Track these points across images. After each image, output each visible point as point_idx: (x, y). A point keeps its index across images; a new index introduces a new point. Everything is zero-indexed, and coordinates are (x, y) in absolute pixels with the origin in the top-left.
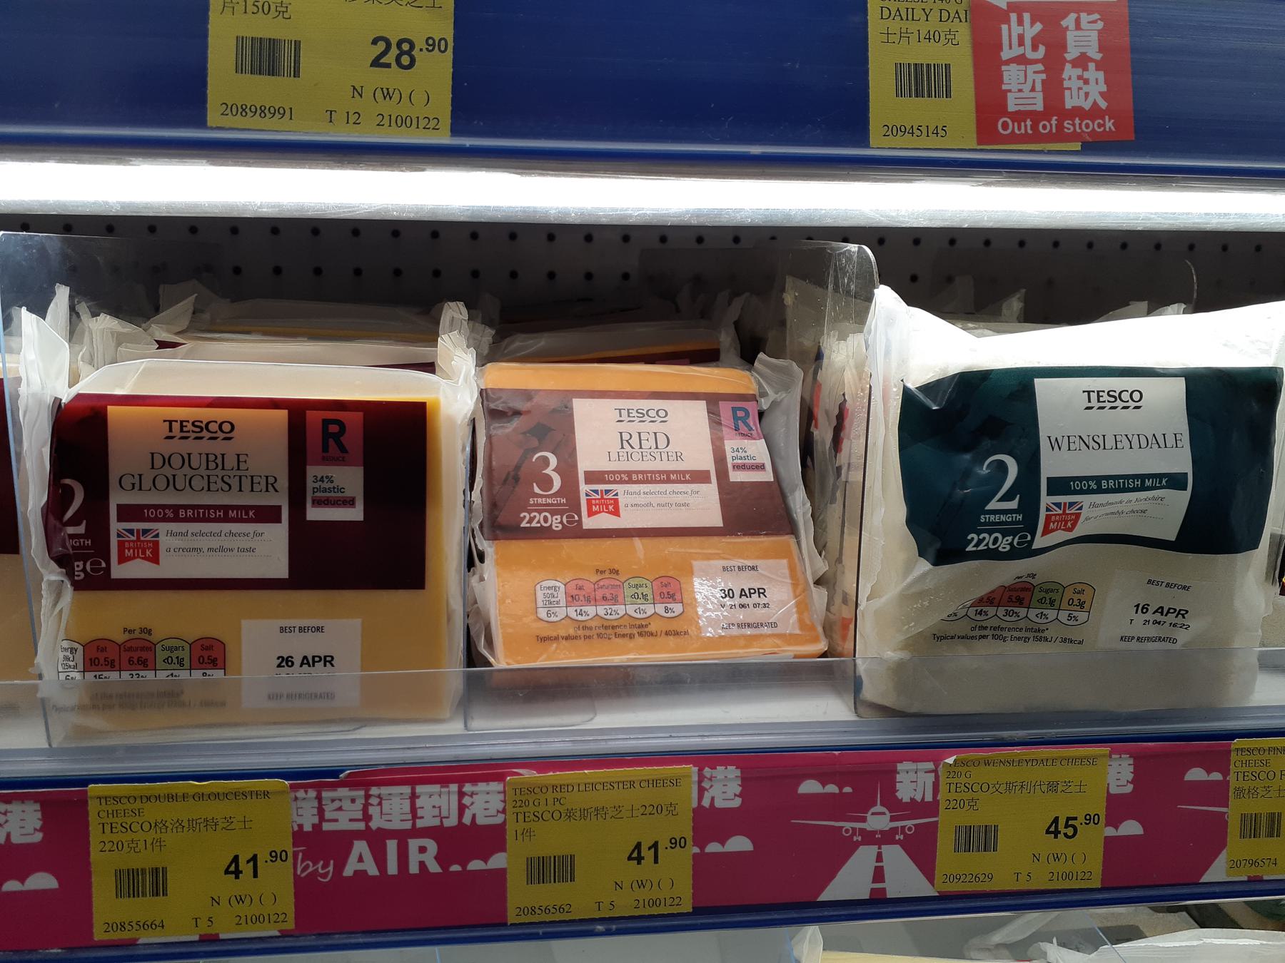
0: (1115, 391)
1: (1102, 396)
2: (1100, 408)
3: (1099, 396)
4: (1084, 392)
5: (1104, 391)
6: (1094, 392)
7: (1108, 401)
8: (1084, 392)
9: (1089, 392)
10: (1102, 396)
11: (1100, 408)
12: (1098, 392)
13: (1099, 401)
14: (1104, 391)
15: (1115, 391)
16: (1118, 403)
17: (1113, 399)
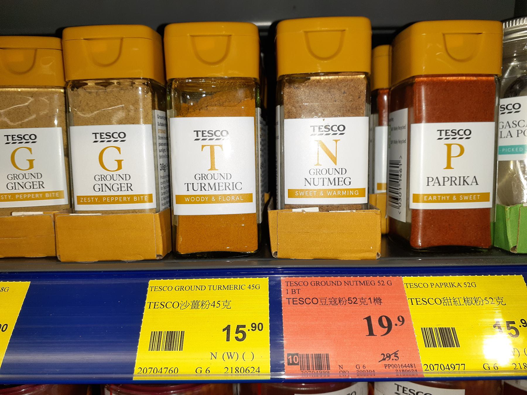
0: (212, 131)
1: (205, 134)
2: (203, 140)
3: (203, 134)
4: (194, 131)
5: (205, 131)
6: (200, 131)
7: (208, 136)
8: (194, 131)
9: (197, 132)
10: (205, 134)
11: (203, 140)
12: (203, 131)
13: (203, 136)
14: (205, 131)
15: (212, 131)
16: (214, 137)
17: (211, 135)
